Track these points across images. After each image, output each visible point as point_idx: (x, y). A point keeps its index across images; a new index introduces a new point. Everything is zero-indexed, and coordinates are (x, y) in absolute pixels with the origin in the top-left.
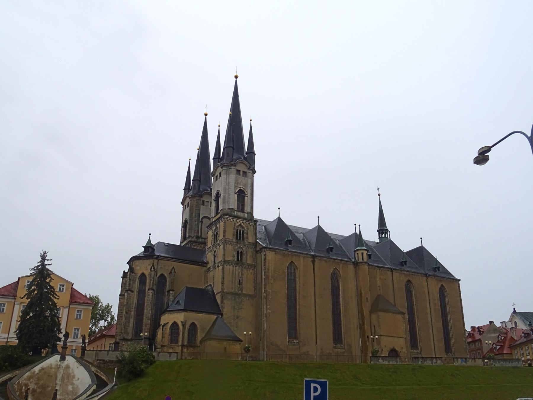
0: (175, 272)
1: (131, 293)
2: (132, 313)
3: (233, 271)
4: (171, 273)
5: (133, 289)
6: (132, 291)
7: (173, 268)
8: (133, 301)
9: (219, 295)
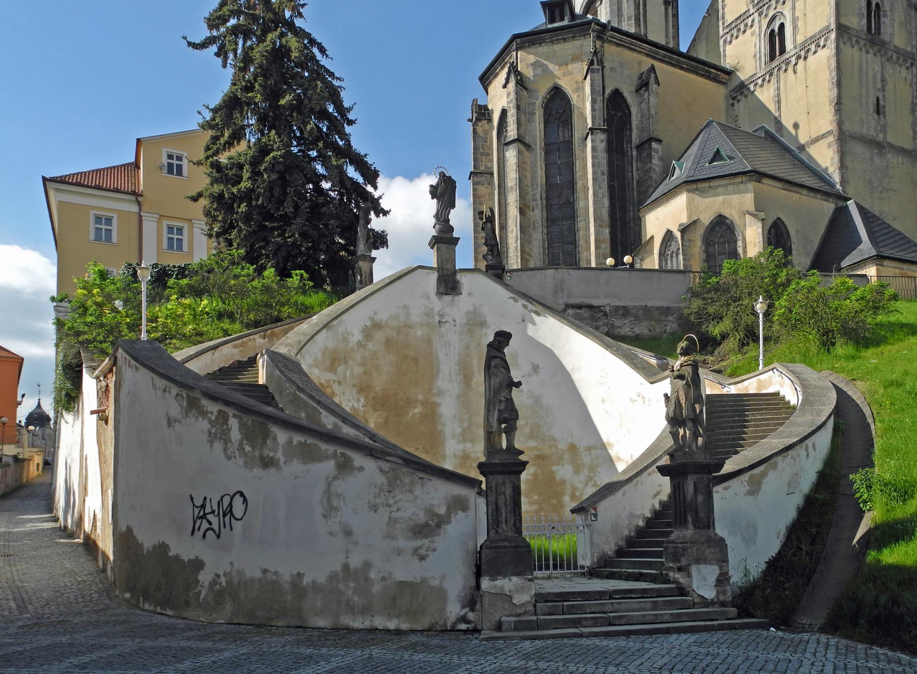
0: (657, 82)
1: (526, 154)
2: (537, 215)
3: (861, 67)
4: (643, 85)
5: (527, 142)
6: (528, 146)
7: (652, 69)
8: (533, 177)
9: (823, 143)
